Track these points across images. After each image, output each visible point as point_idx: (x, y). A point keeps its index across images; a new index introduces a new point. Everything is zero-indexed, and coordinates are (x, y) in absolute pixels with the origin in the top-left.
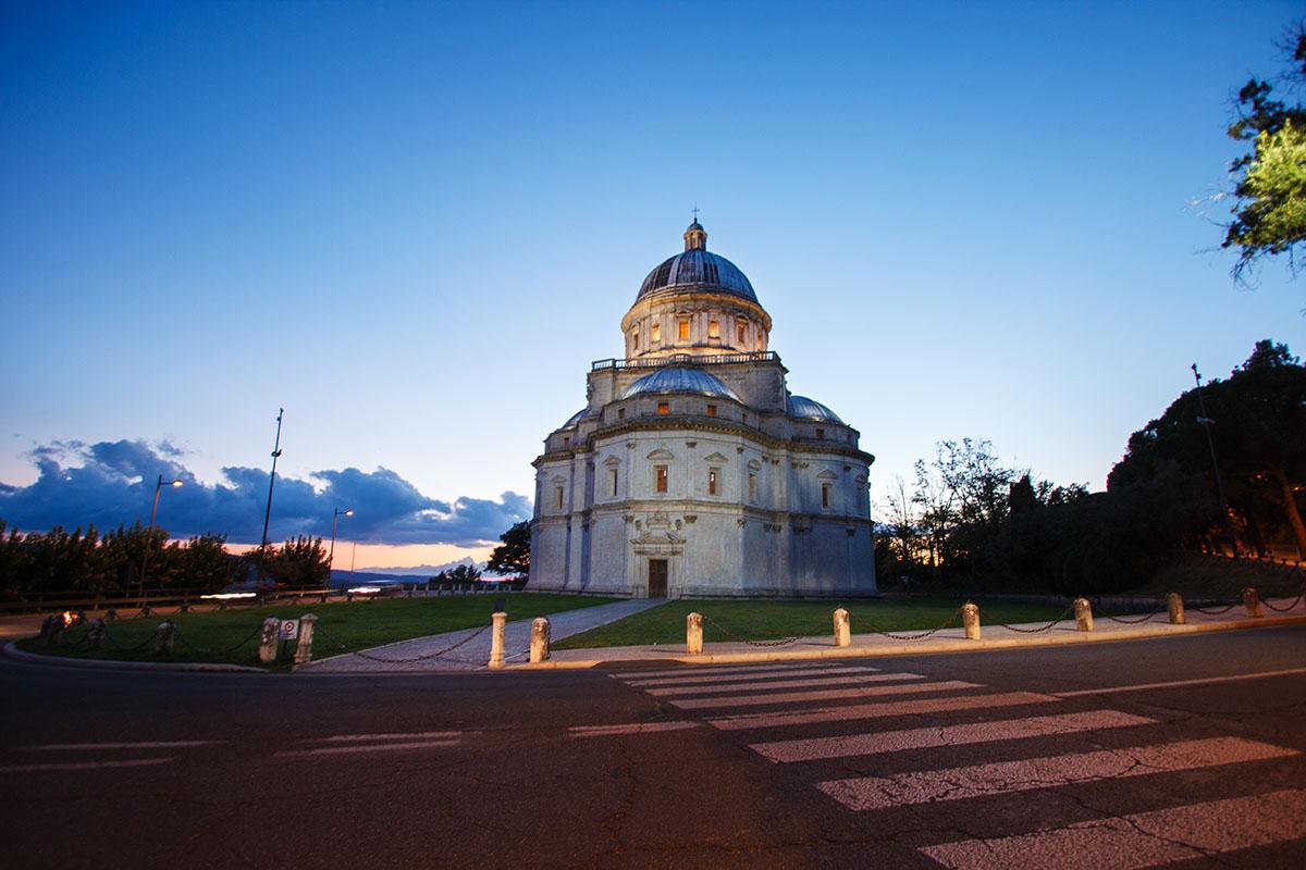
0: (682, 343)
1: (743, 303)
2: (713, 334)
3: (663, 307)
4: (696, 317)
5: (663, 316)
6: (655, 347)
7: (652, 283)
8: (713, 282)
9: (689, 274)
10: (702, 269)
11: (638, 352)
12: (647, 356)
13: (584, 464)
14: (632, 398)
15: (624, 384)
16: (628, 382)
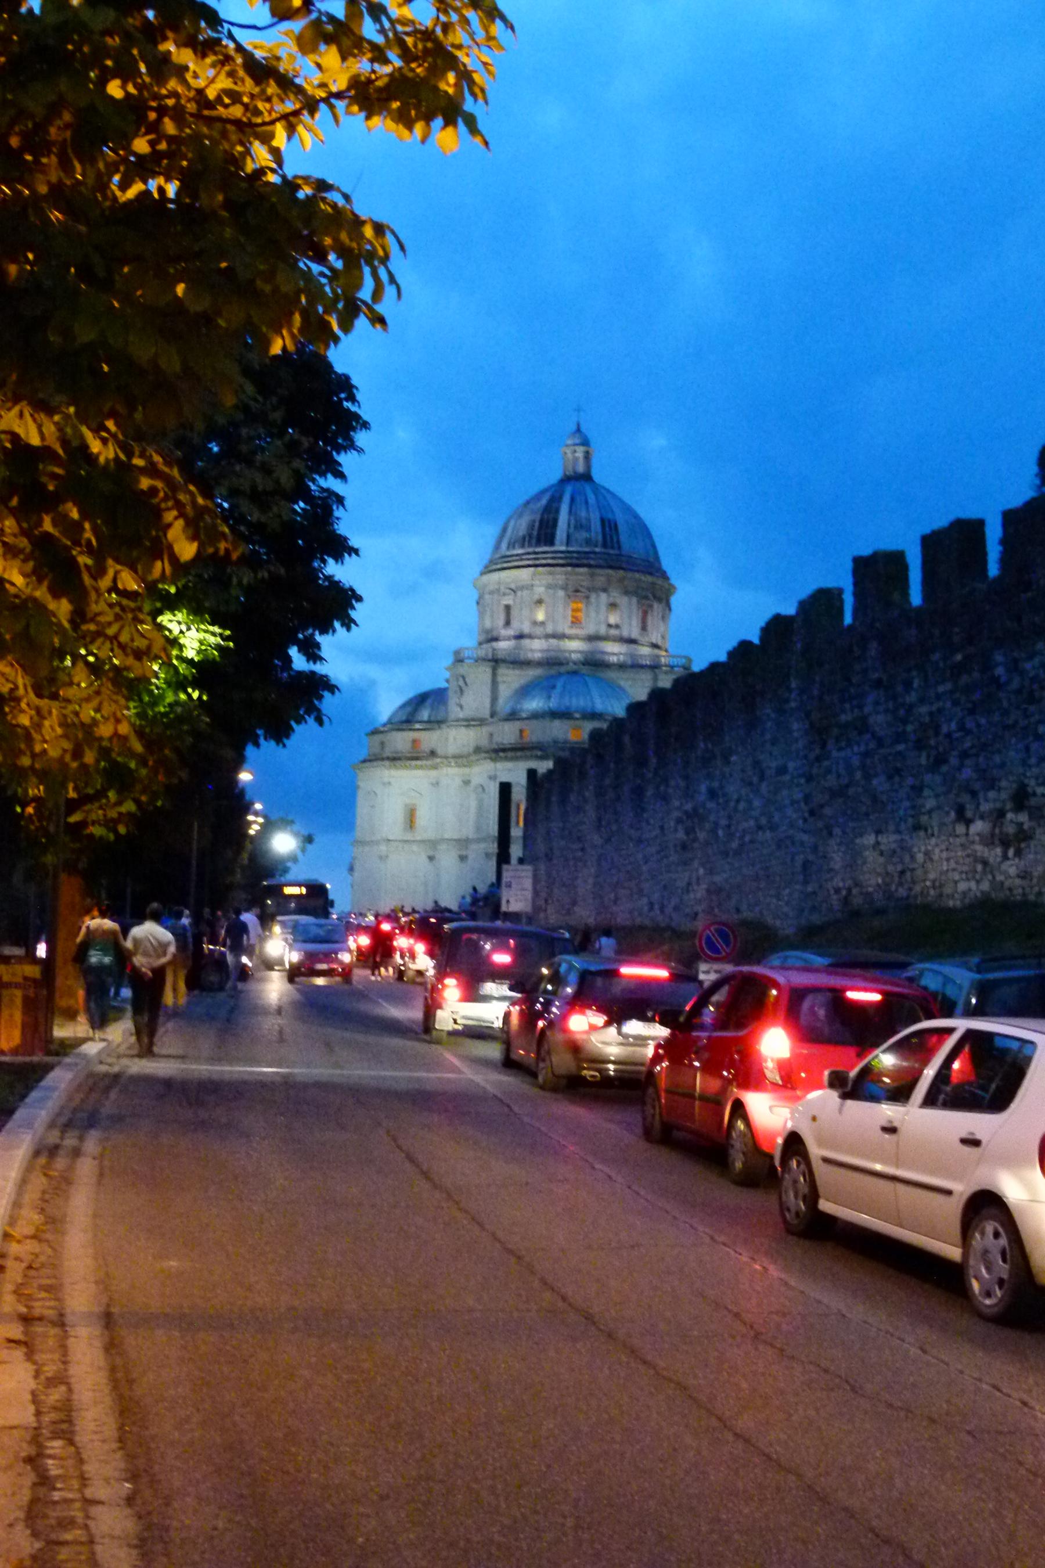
0: (573, 631)
1: (649, 579)
2: (612, 620)
3: (549, 579)
4: (593, 596)
5: (551, 591)
6: (539, 631)
7: (530, 536)
8: (612, 548)
9: (585, 535)
10: (599, 529)
11: (511, 632)
12: (526, 642)
13: (458, 781)
14: (535, 716)
15: (504, 682)
16: (509, 679)
